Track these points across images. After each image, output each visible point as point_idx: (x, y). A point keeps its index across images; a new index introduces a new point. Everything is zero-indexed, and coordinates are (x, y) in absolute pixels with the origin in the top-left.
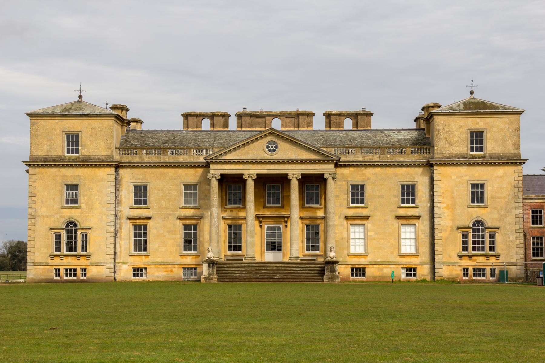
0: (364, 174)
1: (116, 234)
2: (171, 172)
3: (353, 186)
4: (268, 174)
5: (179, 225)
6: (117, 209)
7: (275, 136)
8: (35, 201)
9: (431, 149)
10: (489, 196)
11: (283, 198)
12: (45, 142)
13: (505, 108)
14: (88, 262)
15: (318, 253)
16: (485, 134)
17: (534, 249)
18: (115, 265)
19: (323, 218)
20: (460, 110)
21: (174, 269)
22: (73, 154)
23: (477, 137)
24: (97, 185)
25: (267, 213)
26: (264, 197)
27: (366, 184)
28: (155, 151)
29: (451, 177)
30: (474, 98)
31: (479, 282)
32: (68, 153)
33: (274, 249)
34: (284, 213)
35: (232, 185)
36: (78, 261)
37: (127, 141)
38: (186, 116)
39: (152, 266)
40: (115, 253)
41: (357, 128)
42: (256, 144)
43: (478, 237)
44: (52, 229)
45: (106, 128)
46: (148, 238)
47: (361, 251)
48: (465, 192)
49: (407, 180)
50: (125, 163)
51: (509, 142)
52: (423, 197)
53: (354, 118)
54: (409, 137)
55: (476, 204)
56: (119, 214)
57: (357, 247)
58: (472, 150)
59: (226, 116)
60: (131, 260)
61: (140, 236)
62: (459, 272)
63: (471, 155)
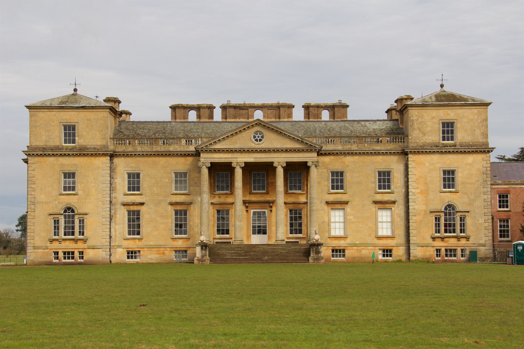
0: (344, 162)
1: (111, 219)
2: (162, 160)
3: (333, 173)
4: (254, 164)
5: (171, 210)
6: (112, 196)
7: (262, 127)
8: (34, 188)
9: (406, 138)
10: (459, 182)
11: (268, 184)
12: (43, 133)
13: (474, 101)
14: (85, 246)
15: (300, 235)
16: (455, 125)
17: (501, 231)
18: (110, 249)
19: (306, 203)
20: (432, 102)
21: (166, 252)
22: (70, 145)
23: (448, 127)
24: (94, 173)
25: (254, 198)
26: (250, 184)
27: (345, 171)
28: (147, 140)
29: (425, 164)
30: (444, 91)
31: (452, 261)
32: (65, 143)
33: (259, 233)
34: (268, 198)
35: (221, 173)
36: (76, 245)
37: (120, 132)
38: (174, 108)
39: (145, 249)
40: (110, 237)
41: (334, 119)
42: (244, 134)
43: (449, 221)
44: (51, 215)
45: (101, 119)
46: (141, 223)
47: (341, 233)
48: (438, 178)
49: (384, 167)
50: (119, 152)
51: (478, 132)
52: (398, 183)
53: (332, 110)
54: (384, 127)
55: (447, 190)
56: (114, 201)
57: (337, 230)
58: (444, 139)
59: (211, 108)
60: (126, 243)
61: (134, 221)
62: (432, 253)
63: (443, 144)
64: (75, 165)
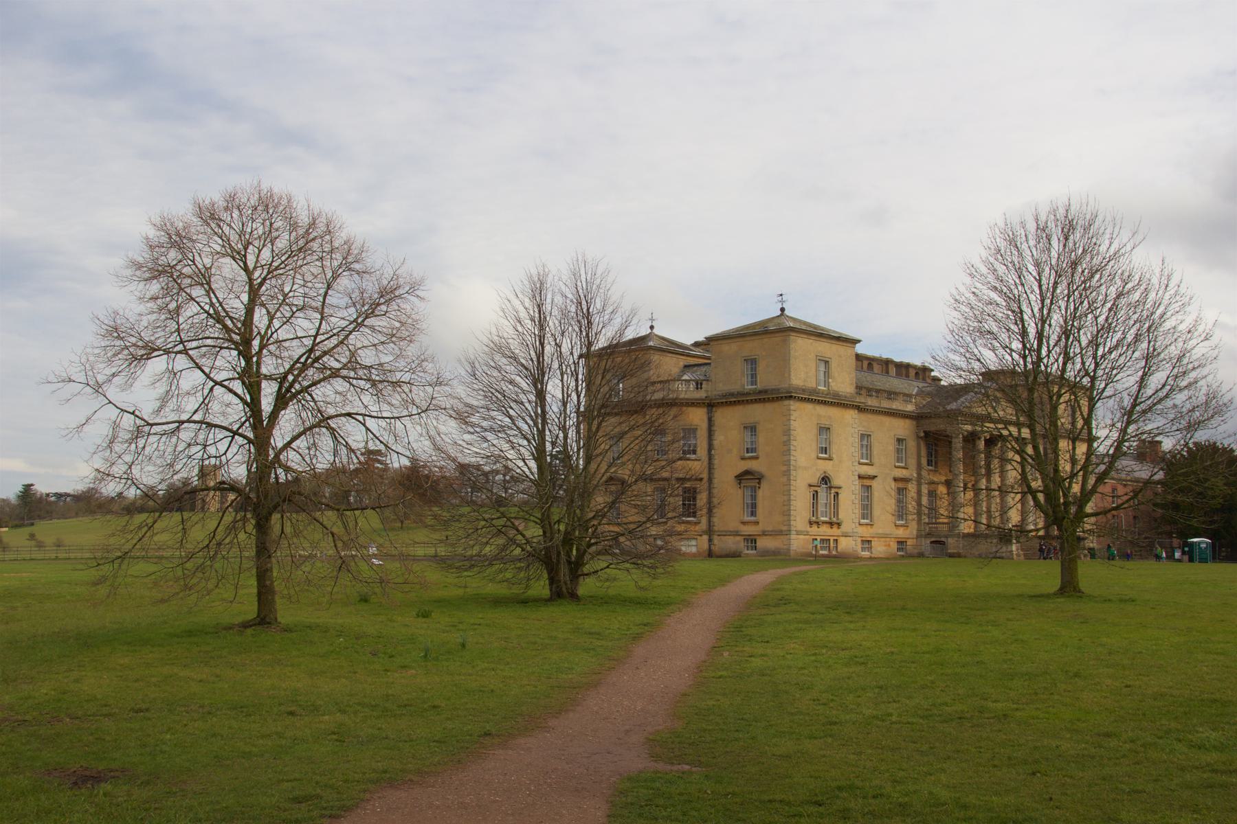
64: (830, 417)
